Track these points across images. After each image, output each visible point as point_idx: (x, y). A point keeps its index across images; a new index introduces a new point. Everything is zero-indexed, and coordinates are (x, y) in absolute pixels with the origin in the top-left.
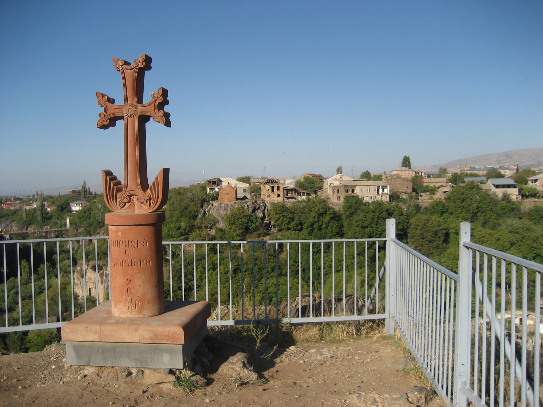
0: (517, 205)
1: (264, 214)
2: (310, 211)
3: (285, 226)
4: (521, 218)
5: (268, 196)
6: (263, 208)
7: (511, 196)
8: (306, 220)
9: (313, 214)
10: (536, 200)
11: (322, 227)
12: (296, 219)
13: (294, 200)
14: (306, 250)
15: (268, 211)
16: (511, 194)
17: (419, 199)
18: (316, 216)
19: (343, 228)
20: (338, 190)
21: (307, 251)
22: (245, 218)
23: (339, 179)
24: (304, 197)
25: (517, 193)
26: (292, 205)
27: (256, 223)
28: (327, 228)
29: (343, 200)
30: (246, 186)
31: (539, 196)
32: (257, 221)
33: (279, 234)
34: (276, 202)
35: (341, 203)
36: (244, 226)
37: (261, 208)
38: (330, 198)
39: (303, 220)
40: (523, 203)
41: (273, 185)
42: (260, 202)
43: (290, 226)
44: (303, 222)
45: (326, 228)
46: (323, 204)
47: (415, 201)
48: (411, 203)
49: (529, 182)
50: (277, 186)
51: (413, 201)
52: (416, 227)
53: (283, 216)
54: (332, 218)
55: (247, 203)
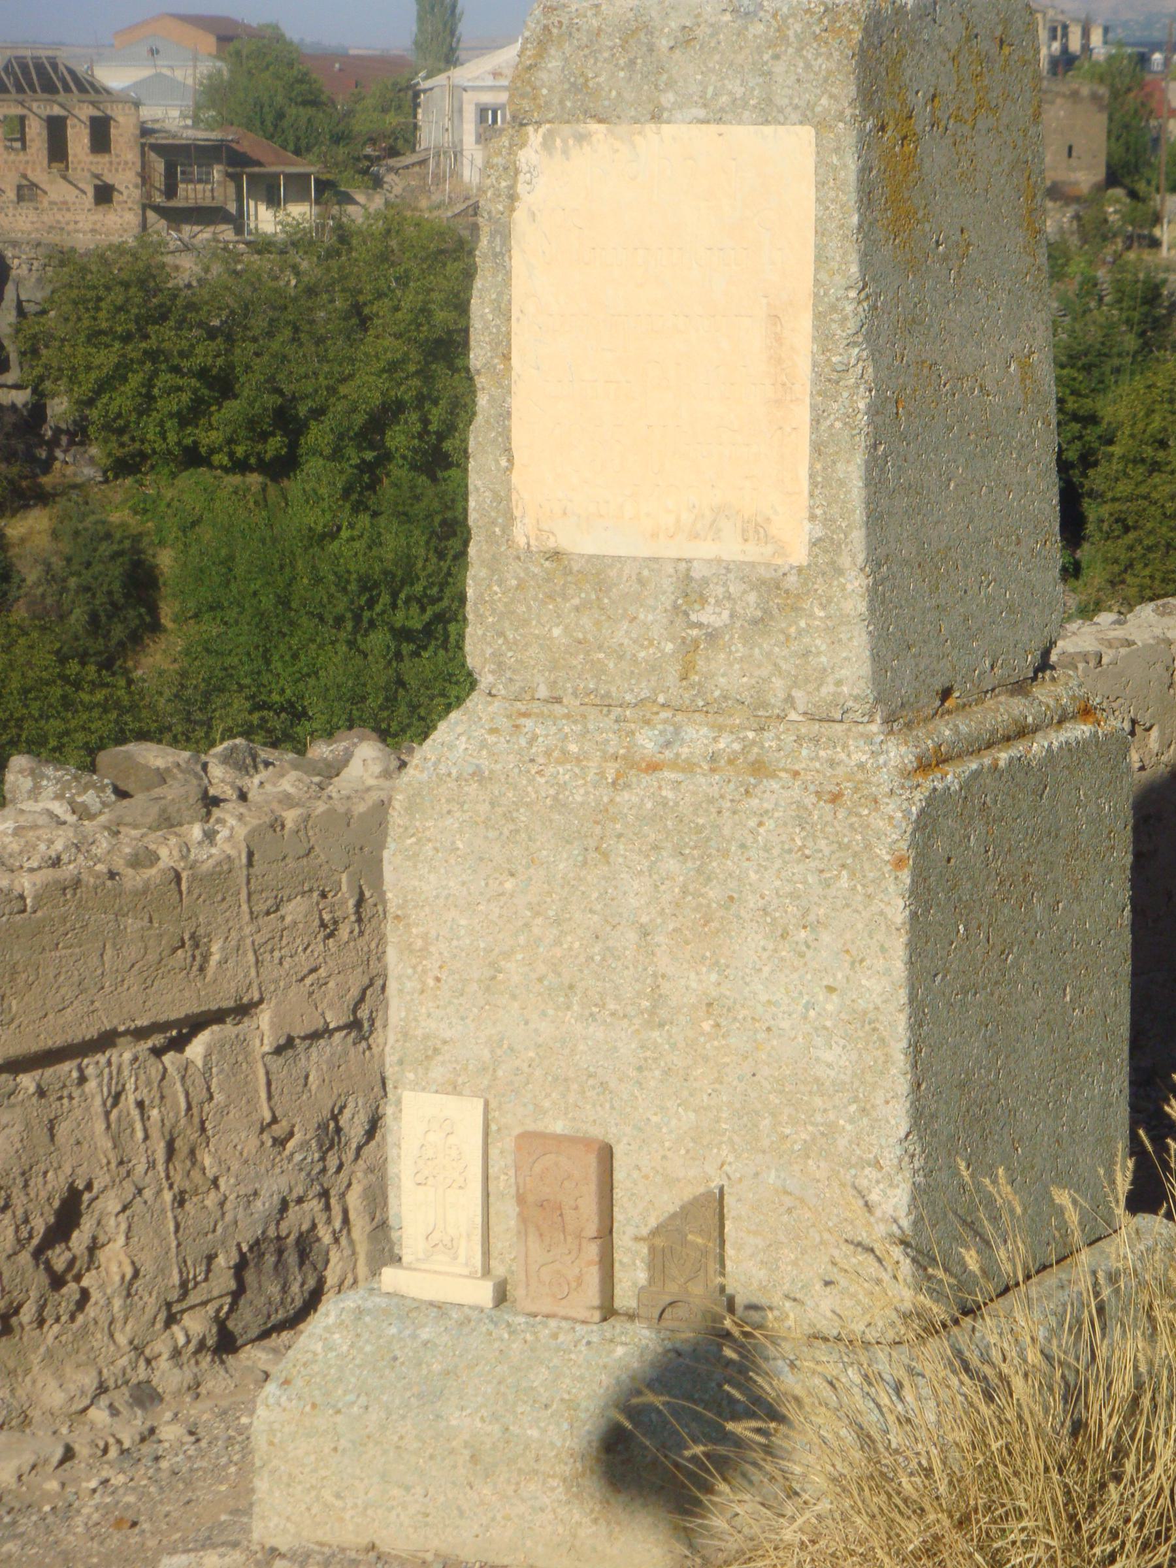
5: (20, 198)
8: (332, 390)
12: (247, 386)
13: (227, 233)
14: (339, 621)
15: (21, 312)
17: (1155, 243)
18: (405, 359)
21: (349, 625)
24: (300, 212)
33: (118, 497)
41: (57, 111)
43: (208, 437)
44: (302, 410)
47: (1131, 256)
48: (1101, 273)
50: (93, 120)
51: (1118, 256)
52: (1149, 452)
53: (152, 356)
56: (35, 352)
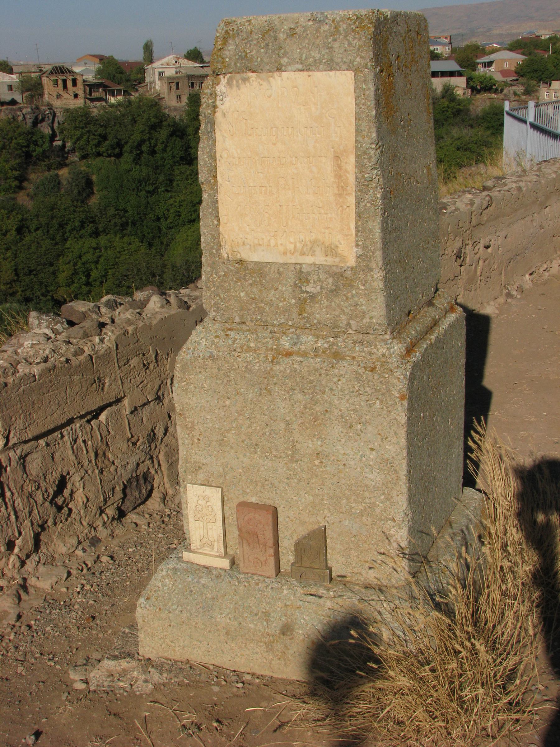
0: (464, 106)
1: (53, 129)
2: (134, 121)
3: (92, 149)
4: (472, 126)
5: (57, 98)
6: (51, 118)
7: (456, 89)
8: (129, 138)
9: (140, 127)
10: (494, 96)
11: (155, 149)
12: (110, 137)
13: (104, 103)
14: (134, 189)
15: (59, 123)
16: (457, 86)
18: (145, 130)
19: (190, 150)
20: (177, 84)
21: (136, 190)
22: (22, 136)
23: (174, 64)
24: (120, 98)
25: (464, 85)
26: (102, 111)
27: (42, 145)
28: (164, 150)
29: (187, 101)
30: (13, 79)
31: (496, 89)
32: (44, 142)
33: (83, 164)
34: (72, 107)
35: (183, 107)
36: (23, 152)
37: (47, 119)
38: (164, 98)
39: (124, 137)
40: (473, 101)
41: (65, 78)
42: (44, 108)
43: (102, 150)
44: (123, 142)
45: (163, 149)
46: (155, 109)
49: (479, 67)
53: (89, 132)
54: (172, 134)
55: (21, 111)
56: (62, 132)
